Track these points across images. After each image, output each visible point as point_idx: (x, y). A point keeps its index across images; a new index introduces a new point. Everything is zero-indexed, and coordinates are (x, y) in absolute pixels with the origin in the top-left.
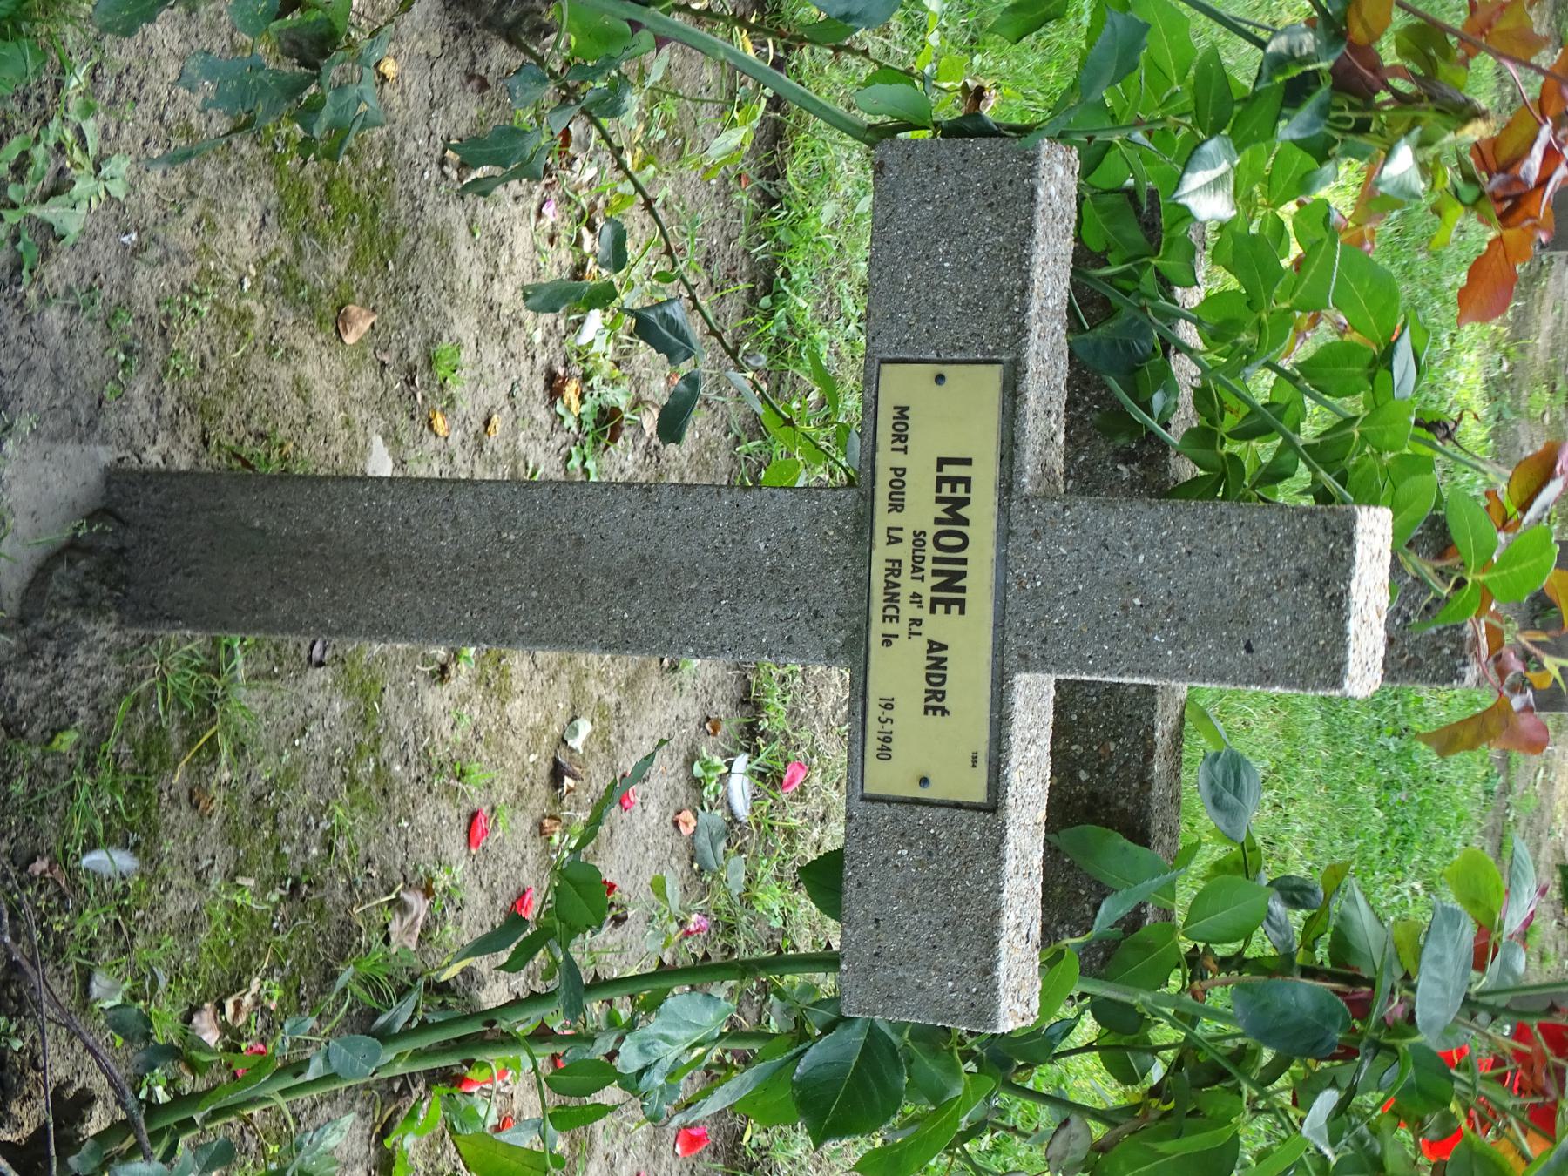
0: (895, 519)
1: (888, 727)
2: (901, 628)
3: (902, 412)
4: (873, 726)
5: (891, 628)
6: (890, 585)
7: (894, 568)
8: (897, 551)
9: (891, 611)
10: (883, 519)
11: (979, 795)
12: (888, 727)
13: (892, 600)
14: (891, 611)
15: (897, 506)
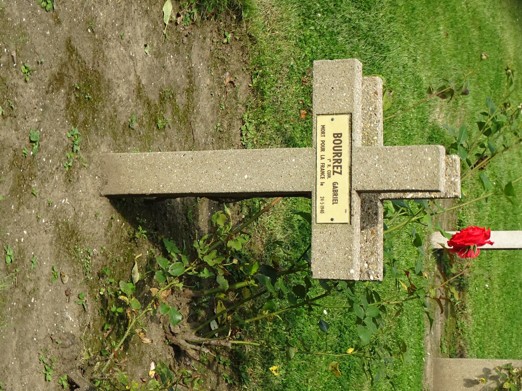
0: (323, 153)
1: (323, 205)
2: (325, 180)
3: (323, 127)
4: (319, 205)
5: (322, 180)
6: (322, 170)
7: (323, 166)
8: (323, 161)
9: (323, 176)
10: (319, 153)
11: (347, 221)
12: (323, 205)
13: (323, 173)
14: (323, 176)
15: (323, 150)
